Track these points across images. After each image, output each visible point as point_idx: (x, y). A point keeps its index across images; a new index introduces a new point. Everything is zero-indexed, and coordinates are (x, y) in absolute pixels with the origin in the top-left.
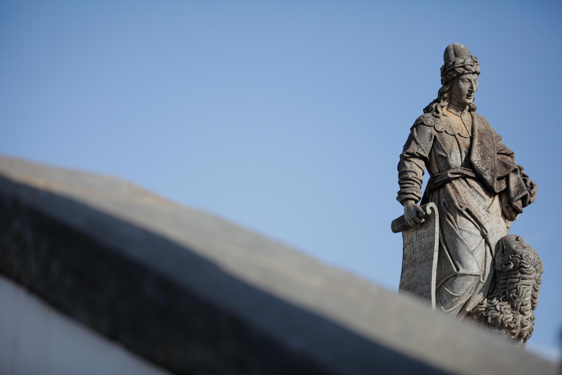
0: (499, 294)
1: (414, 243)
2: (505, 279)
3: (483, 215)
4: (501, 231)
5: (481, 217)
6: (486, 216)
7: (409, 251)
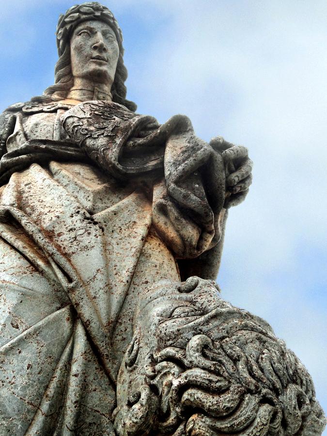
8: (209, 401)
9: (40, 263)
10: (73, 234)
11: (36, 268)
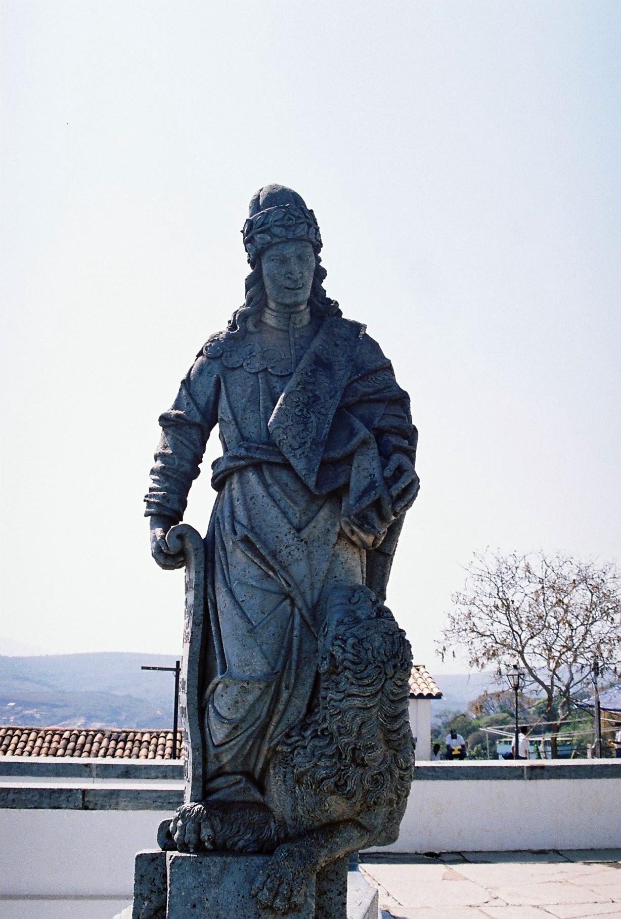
3: (287, 547)
4: (336, 577)
6: (293, 548)
8: (352, 667)
9: (271, 573)
10: (288, 550)
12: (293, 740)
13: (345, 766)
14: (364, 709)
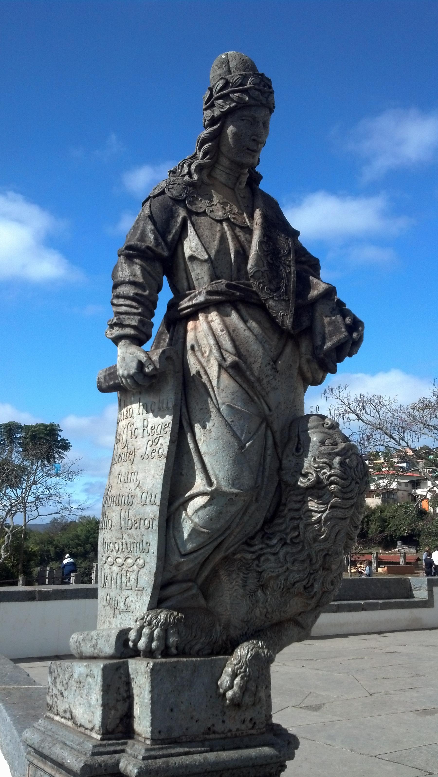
0: (286, 529)
1: (135, 418)
2: (300, 502)
3: (267, 376)
5: (262, 380)
6: (271, 377)
7: (126, 430)
9: (256, 398)
11: (253, 400)
12: (256, 548)
13: (314, 570)
14: (342, 519)
